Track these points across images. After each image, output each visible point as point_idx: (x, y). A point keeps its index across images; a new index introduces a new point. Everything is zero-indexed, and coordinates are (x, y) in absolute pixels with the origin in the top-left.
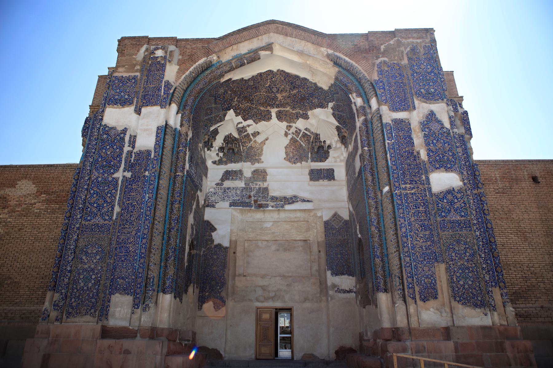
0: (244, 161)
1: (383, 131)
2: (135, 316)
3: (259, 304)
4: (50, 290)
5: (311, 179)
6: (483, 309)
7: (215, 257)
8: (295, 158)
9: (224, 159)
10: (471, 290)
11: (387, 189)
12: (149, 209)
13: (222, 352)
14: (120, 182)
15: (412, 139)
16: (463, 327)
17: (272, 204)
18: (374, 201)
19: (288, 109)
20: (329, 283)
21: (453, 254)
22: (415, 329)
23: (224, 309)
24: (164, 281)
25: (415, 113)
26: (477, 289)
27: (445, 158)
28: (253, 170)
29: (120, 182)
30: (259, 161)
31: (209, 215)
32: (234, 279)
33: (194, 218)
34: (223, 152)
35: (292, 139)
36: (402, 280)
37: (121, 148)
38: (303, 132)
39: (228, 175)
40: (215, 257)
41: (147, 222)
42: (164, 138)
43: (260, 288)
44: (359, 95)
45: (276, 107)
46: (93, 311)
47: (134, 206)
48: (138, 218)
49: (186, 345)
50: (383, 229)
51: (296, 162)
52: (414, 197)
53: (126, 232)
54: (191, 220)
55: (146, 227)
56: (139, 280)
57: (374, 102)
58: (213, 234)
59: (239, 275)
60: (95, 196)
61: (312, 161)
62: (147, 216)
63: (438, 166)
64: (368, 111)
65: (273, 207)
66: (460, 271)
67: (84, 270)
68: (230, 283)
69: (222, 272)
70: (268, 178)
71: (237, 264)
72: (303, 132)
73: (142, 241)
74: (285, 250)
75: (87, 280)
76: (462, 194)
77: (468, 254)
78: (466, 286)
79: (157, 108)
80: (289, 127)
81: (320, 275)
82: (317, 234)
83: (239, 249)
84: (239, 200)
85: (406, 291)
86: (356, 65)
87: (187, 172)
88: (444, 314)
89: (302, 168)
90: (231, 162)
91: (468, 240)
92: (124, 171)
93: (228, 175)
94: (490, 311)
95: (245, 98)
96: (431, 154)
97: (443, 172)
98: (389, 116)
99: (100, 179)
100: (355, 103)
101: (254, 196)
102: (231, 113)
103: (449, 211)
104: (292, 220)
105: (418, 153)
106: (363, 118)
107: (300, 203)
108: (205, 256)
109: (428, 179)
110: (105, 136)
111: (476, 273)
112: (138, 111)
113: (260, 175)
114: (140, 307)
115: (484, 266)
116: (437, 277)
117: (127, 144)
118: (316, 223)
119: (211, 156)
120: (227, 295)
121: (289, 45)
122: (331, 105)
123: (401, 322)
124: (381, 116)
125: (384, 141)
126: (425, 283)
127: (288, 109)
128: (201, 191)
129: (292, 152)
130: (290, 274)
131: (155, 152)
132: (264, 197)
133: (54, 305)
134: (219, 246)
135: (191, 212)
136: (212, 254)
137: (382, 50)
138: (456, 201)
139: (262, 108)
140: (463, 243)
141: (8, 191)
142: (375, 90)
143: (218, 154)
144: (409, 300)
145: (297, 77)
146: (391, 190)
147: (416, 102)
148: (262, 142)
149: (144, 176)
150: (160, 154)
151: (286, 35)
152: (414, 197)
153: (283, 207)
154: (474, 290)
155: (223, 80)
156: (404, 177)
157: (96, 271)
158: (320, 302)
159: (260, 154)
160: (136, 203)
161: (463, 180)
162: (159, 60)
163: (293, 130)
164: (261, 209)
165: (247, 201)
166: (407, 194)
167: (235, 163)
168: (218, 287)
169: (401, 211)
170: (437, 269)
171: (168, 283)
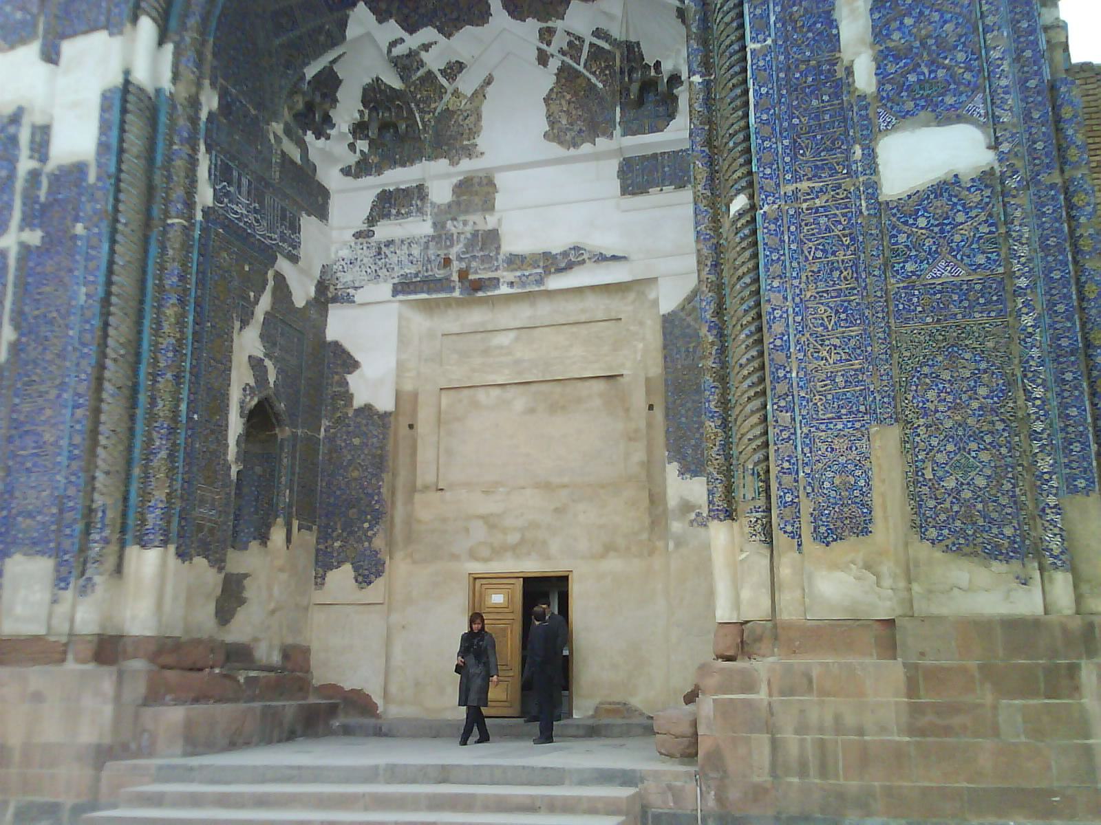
0: (429, 158)
1: (741, 15)
3: (478, 568)
5: (625, 191)
6: (1016, 566)
7: (356, 441)
8: (576, 128)
9: (373, 159)
10: (980, 506)
11: (739, 203)
12: (87, 327)
13: (378, 700)
14: (12, 262)
15: (832, 23)
17: (510, 276)
18: (709, 244)
20: (672, 502)
21: (931, 395)
22: (789, 626)
23: (379, 583)
24: (142, 514)
26: (1004, 501)
27: (941, 73)
28: (455, 180)
29: (12, 262)
30: (470, 152)
31: (339, 326)
32: (410, 500)
33: (263, 337)
34: (367, 137)
35: (561, 70)
36: (767, 481)
37: (12, 162)
38: (591, 45)
40: (356, 441)
41: (84, 363)
42: (123, 122)
43: (480, 523)
47: (51, 322)
49: (247, 679)
51: (578, 140)
52: (823, 220)
53: (35, 395)
54: (248, 342)
55: (83, 376)
56: (69, 516)
58: (349, 378)
59: (426, 488)
61: (624, 134)
62: (84, 345)
63: (910, 105)
65: (511, 284)
66: (950, 447)
68: (399, 513)
69: (373, 481)
70: (500, 200)
71: (420, 458)
72: (591, 45)
73: (73, 415)
74: (555, 408)
76: (988, 192)
77: (982, 391)
78: (967, 494)
79: (100, 37)
80: (546, 35)
81: (650, 477)
82: (641, 357)
84: (416, 275)
85: (774, 513)
87: (206, 212)
88: (887, 582)
89: (597, 157)
90: (394, 163)
91: (990, 344)
92: (21, 229)
94: (1042, 569)
96: (891, 68)
97: (927, 125)
101: (460, 259)
103: (933, 255)
104: (572, 320)
105: (849, 71)
107: (589, 264)
108: (331, 439)
111: (1004, 451)
113: (476, 192)
114: (71, 586)
115: (1039, 426)
116: (875, 469)
118: (641, 324)
119: (331, 154)
120: (391, 544)
123: (755, 606)
126: (835, 488)
128: (294, 259)
129: (568, 113)
130: (566, 480)
131: (100, 166)
132: (484, 259)
134: (368, 409)
135: (245, 323)
136: (348, 433)
138: (960, 217)
140: (967, 356)
143: (352, 147)
144: (780, 538)
146: (753, 207)
148: (475, 93)
149: (75, 237)
150: (112, 169)
152: (823, 220)
153: (540, 281)
154: (991, 506)
156: (794, 158)
158: (651, 553)
159: (474, 132)
160: (55, 314)
161: (995, 145)
163: (560, 41)
164: (480, 294)
165: (440, 274)
166: (798, 213)
167: (403, 165)
168: (366, 525)
169: (776, 269)
170: (877, 443)
171: (153, 518)
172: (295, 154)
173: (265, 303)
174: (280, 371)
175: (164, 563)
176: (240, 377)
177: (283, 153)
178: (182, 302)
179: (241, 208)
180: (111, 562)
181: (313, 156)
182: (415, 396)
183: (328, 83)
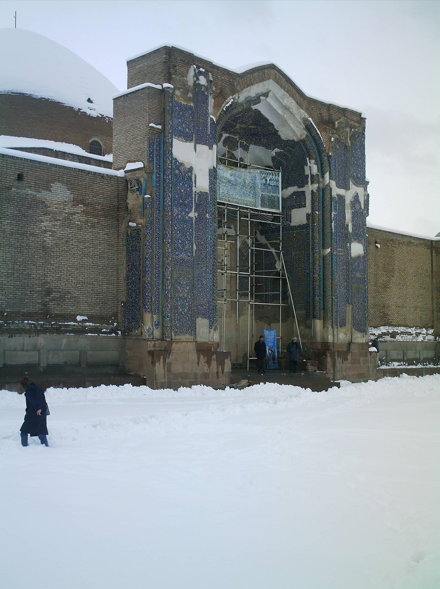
1: (331, 203)
2: (211, 334)
4: (148, 312)
11: (329, 250)
16: (355, 343)
19: (236, 137)
25: (349, 191)
44: (316, 163)
45: (229, 134)
46: (190, 330)
48: (206, 257)
50: (322, 276)
57: (327, 175)
60: (178, 232)
64: (321, 180)
67: (181, 298)
79: (206, 147)
88: (348, 335)
92: (195, 212)
98: (336, 191)
99: (180, 217)
100: (310, 167)
105: (348, 226)
106: (317, 185)
109: (350, 247)
110: (177, 172)
117: (194, 185)
121: (280, 98)
122: (277, 150)
124: (331, 190)
125: (331, 211)
127: (236, 137)
133: (155, 325)
137: (336, 126)
141: (43, 195)
142: (330, 166)
145: (266, 120)
147: (351, 183)
151: (281, 87)
157: (188, 300)
161: (364, 250)
162: (203, 89)
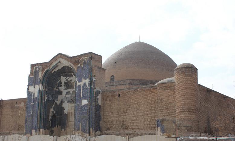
0: (70, 89)
39: (68, 93)
68: (68, 124)
75: (28, 127)
83: (70, 114)
86: (74, 67)
93: (68, 93)
95: (64, 72)
102: (62, 77)
112: (34, 87)
134: (65, 114)
135: (51, 108)
139: (70, 74)
141: (20, 105)
155: (52, 73)
165: (71, 101)
172: (57, 90)
173: (54, 105)
174: (56, 111)
175: (43, 130)
176: (51, 113)
177: (56, 91)
178: (44, 109)
179: (50, 98)
180: (39, 130)
181: (60, 89)
182: (69, 112)
183: (61, 82)
